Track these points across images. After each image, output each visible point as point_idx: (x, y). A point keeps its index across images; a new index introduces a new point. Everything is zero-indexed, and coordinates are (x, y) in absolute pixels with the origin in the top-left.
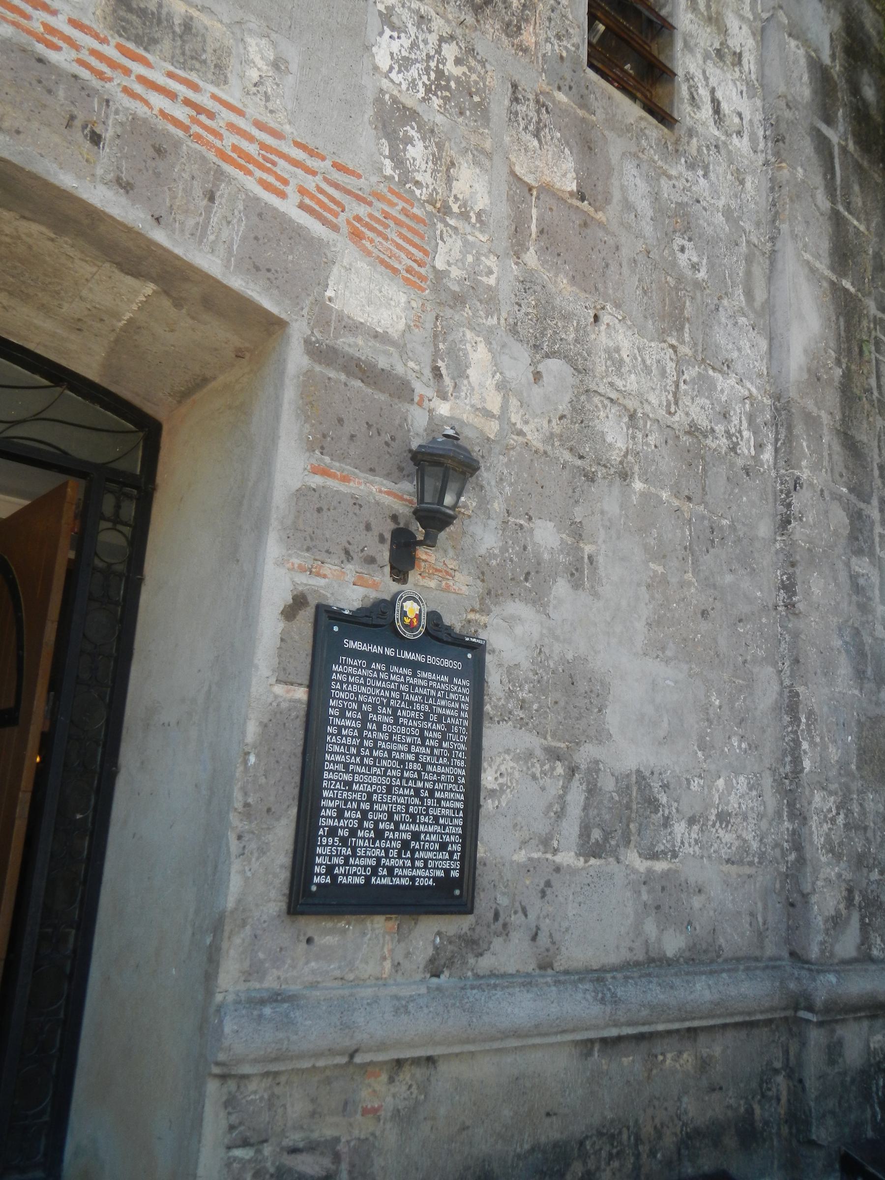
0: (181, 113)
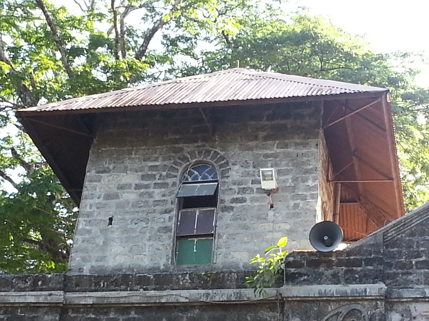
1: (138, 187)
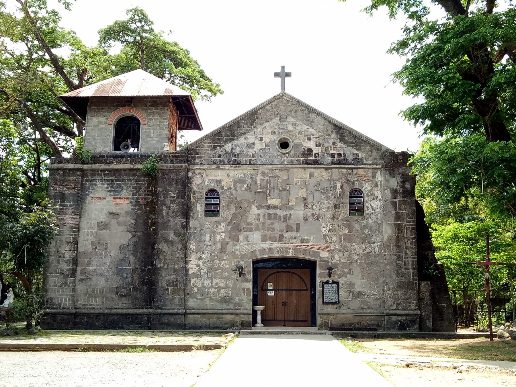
0: (306, 247)
1: (105, 122)
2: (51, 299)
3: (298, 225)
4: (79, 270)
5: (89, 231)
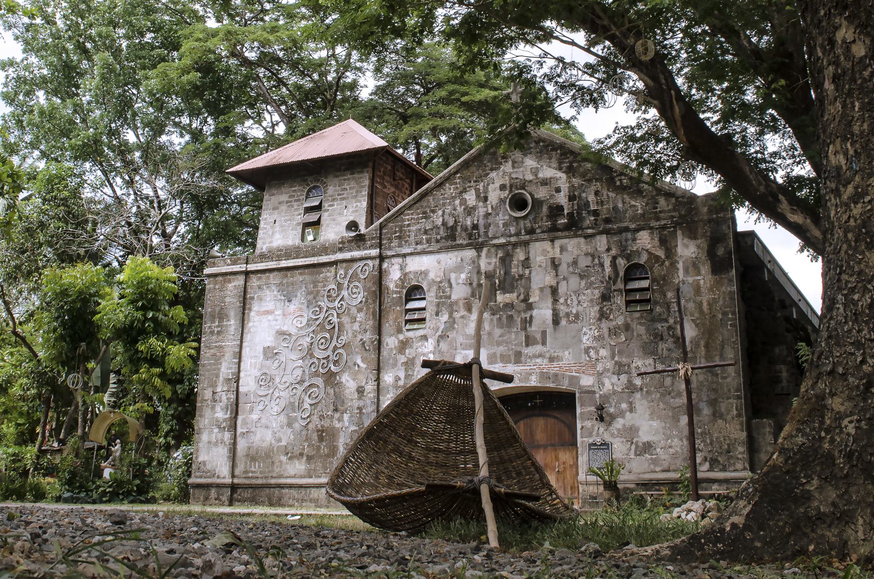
2: (204, 463)
3: (544, 333)
4: (240, 418)
5: (253, 361)
